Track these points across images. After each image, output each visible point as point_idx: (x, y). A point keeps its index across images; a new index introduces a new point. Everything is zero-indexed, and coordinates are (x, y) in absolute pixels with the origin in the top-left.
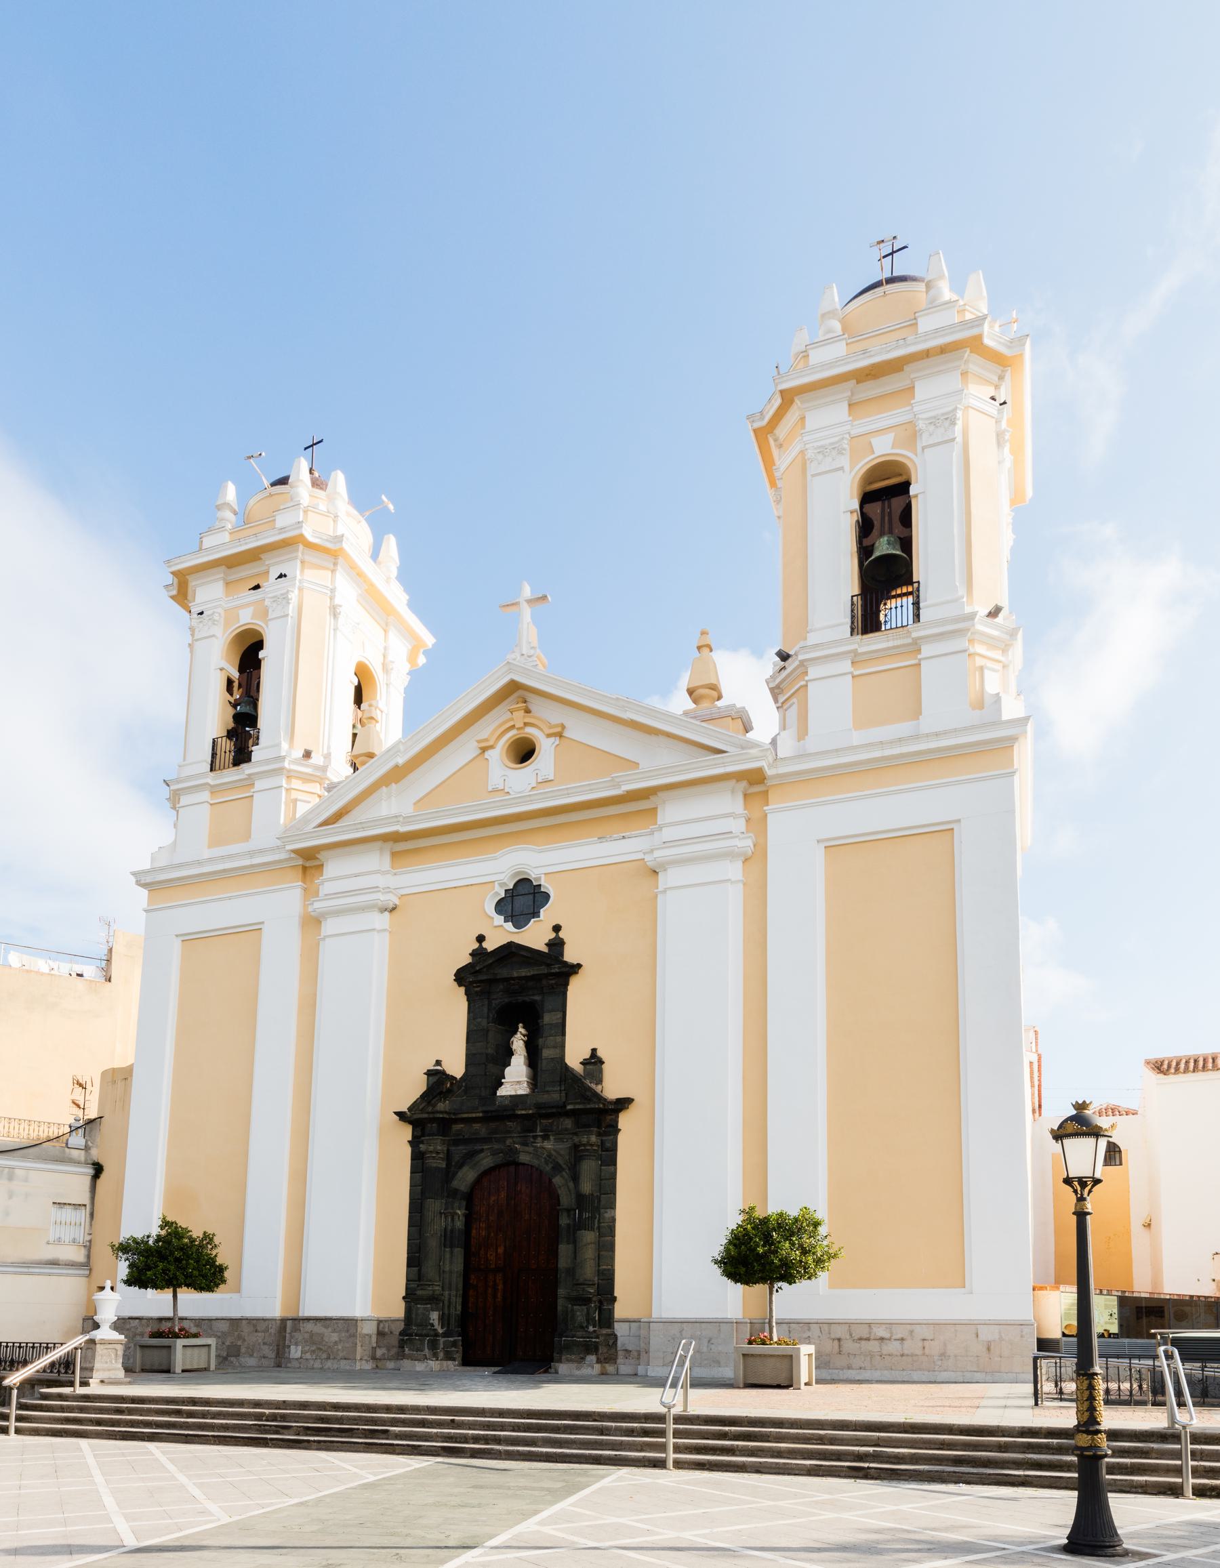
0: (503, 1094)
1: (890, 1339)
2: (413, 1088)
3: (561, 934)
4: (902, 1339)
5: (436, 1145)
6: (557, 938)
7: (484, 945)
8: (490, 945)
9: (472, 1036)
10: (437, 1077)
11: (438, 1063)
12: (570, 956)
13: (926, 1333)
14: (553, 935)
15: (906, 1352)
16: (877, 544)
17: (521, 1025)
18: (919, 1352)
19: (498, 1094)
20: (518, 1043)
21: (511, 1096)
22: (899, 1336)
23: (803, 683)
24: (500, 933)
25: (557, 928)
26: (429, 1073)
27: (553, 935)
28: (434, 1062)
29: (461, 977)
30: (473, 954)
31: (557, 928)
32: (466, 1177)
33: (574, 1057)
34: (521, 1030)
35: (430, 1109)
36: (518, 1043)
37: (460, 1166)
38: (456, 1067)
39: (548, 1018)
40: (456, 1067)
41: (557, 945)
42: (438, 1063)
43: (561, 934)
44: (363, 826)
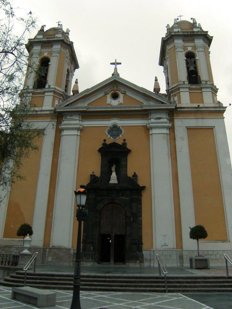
0: (111, 183)
1: (213, 255)
3: (126, 142)
4: (216, 255)
6: (124, 142)
7: (106, 142)
8: (108, 142)
9: (102, 166)
10: (93, 177)
11: (93, 172)
12: (129, 147)
13: (221, 253)
14: (123, 142)
15: (217, 258)
16: (190, 67)
17: (114, 164)
18: (220, 258)
19: (110, 183)
21: (113, 183)
22: (215, 254)
23: (179, 92)
24: (110, 140)
25: (124, 140)
26: (91, 176)
27: (123, 142)
29: (100, 150)
30: (103, 144)
38: (98, 174)
39: (123, 163)
40: (98, 174)
41: (125, 144)
43: (126, 142)
44: (78, 108)
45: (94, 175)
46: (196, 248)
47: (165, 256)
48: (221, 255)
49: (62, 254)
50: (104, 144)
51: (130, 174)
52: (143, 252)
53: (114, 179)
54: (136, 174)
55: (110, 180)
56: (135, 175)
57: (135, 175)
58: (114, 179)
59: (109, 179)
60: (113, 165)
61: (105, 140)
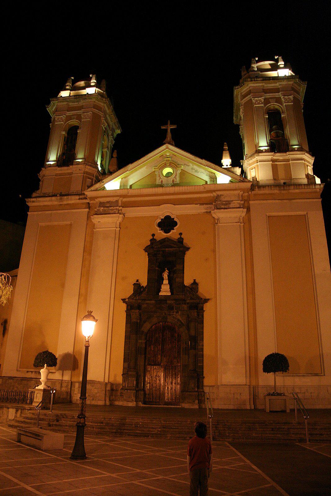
2: (129, 291)
3: (182, 236)
5: (135, 313)
7: (155, 237)
9: (150, 271)
10: (137, 286)
20: (165, 275)
24: (161, 234)
25: (181, 234)
27: (179, 236)
28: (136, 280)
30: (151, 240)
31: (181, 234)
32: (147, 327)
33: (188, 281)
34: (166, 271)
35: (135, 298)
36: (165, 275)
37: (145, 322)
38: (144, 283)
40: (144, 283)
42: (137, 281)
43: (182, 236)
45: (139, 285)
46: (272, 383)
47: (234, 394)
48: (311, 393)
49: (96, 391)
50: (153, 241)
51: (188, 281)
52: (204, 388)
53: (165, 290)
54: (197, 281)
55: (160, 291)
56: (195, 283)
57: (195, 283)
58: (165, 290)
59: (159, 290)
60: (165, 270)
61: (153, 235)
